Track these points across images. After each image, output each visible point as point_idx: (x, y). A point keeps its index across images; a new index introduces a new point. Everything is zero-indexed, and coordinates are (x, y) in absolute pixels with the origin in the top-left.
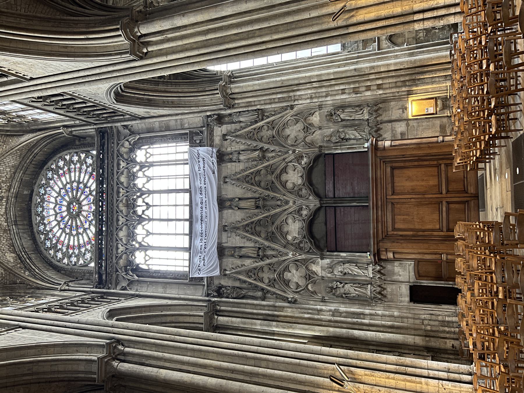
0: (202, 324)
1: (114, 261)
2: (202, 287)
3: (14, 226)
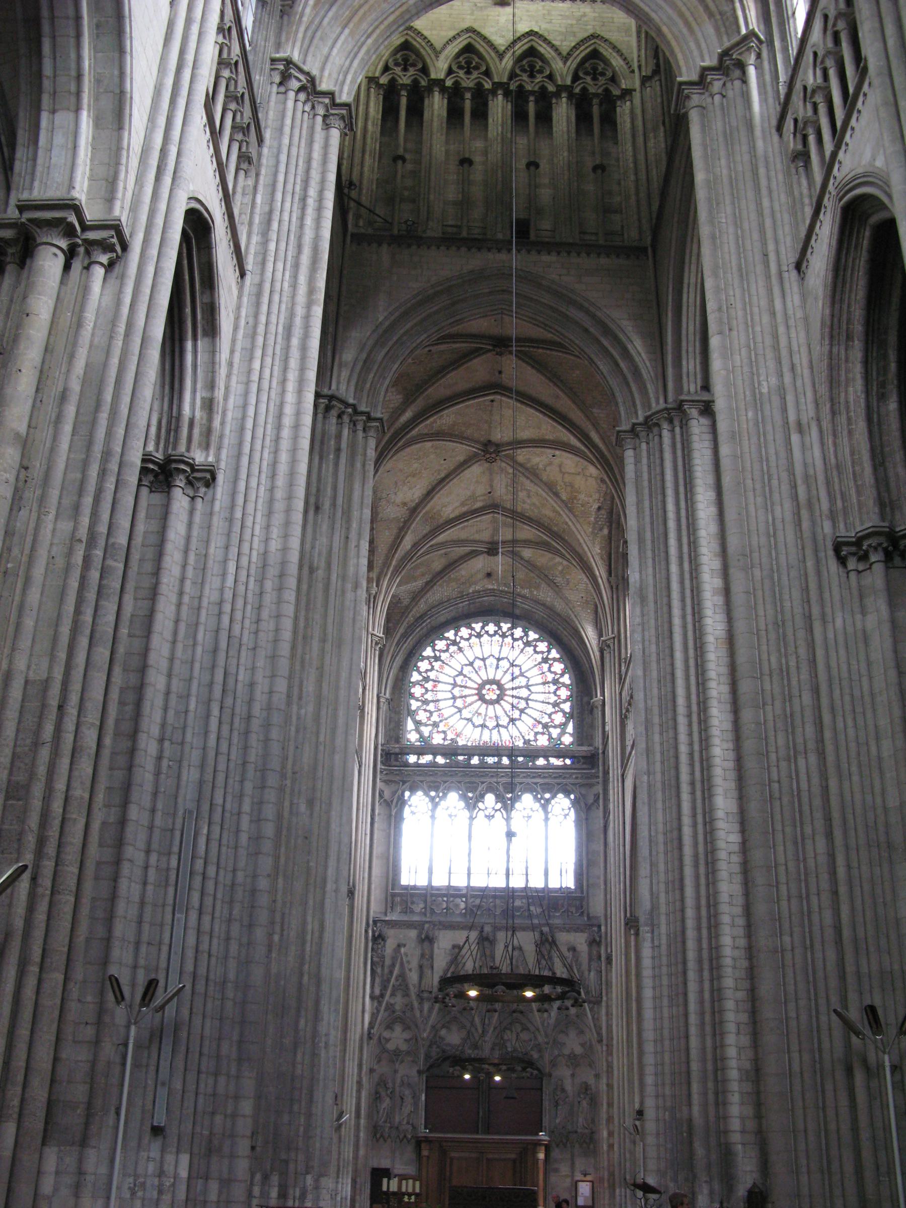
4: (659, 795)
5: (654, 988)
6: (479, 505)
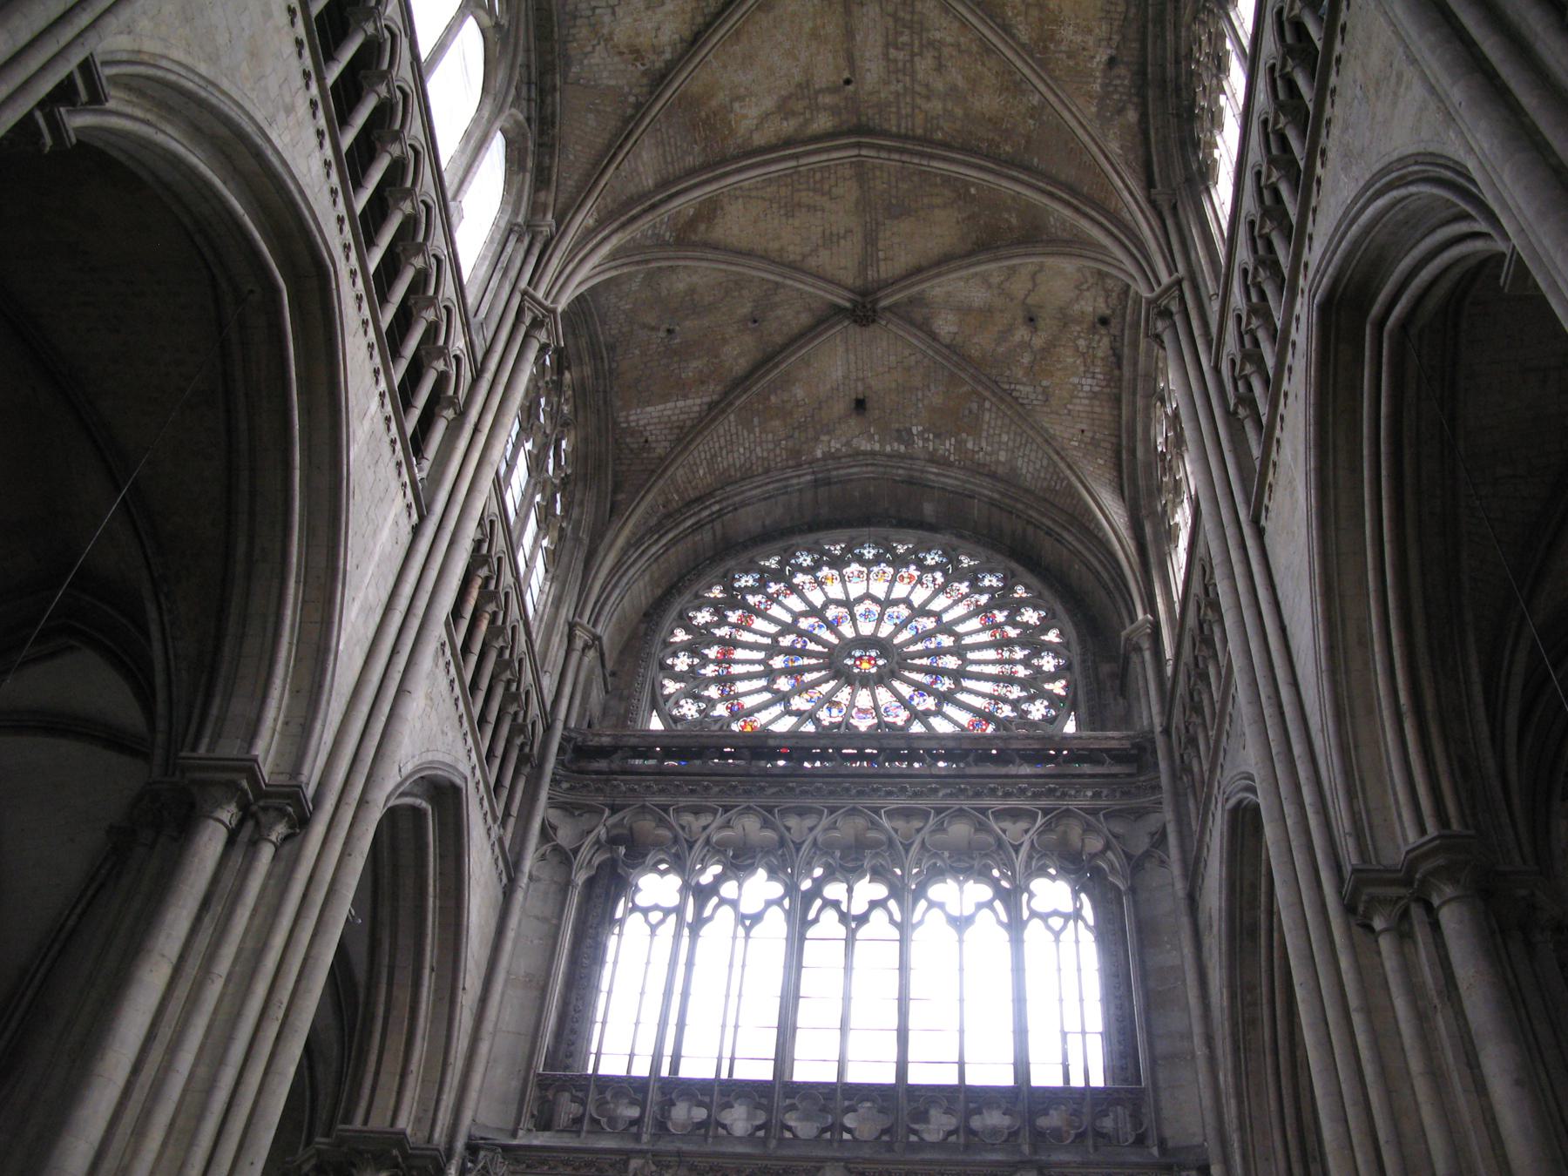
0: (366, 1122)
1: (651, 801)
2: (511, 1126)
3: (809, 478)
6: (823, 122)
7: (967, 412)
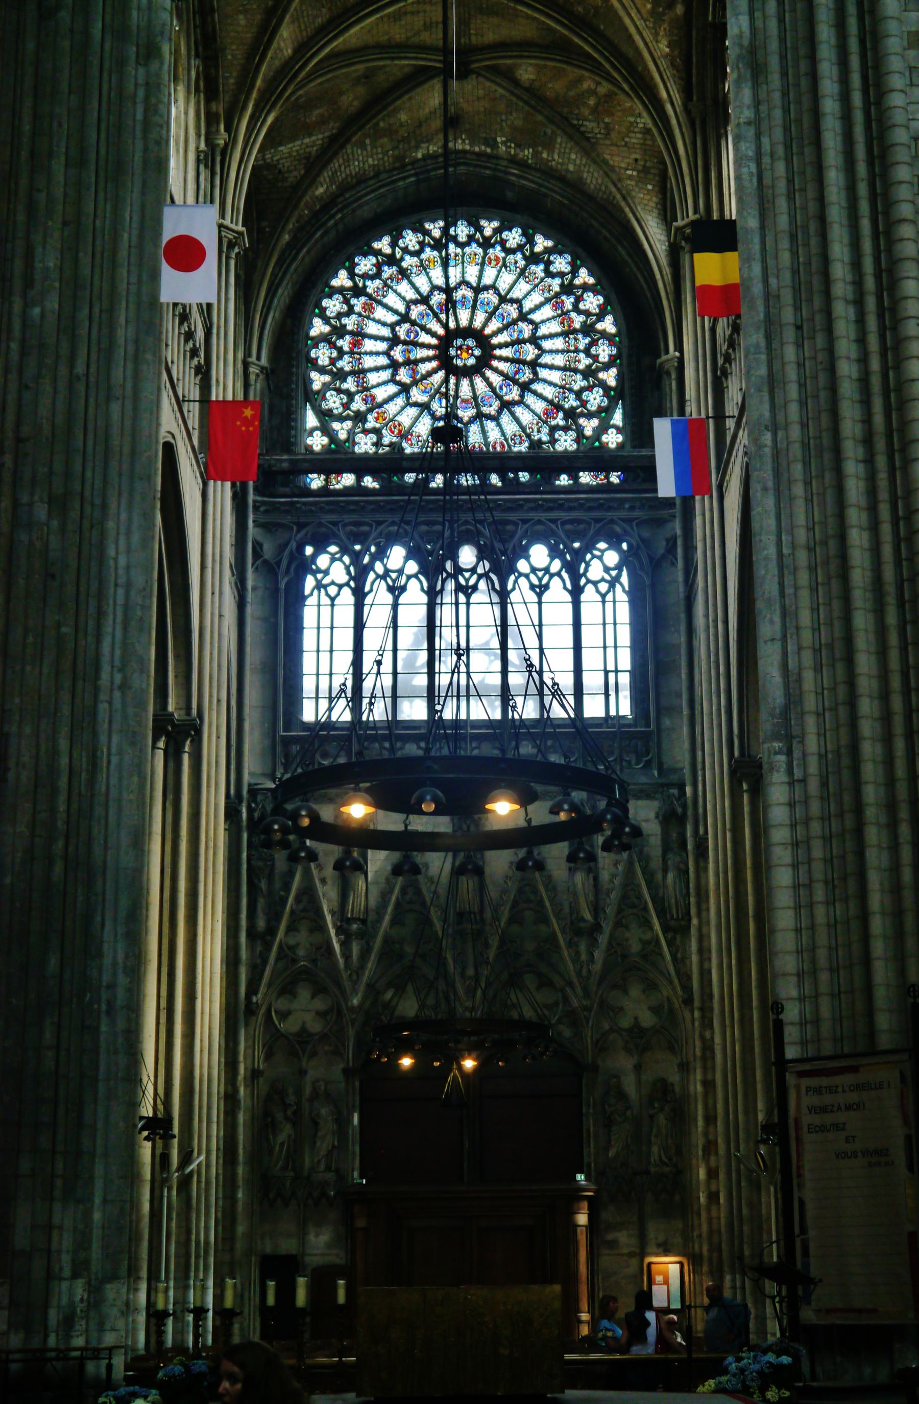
3: (413, 179)
4: (797, 470)
5: (795, 866)
7: (542, 134)
